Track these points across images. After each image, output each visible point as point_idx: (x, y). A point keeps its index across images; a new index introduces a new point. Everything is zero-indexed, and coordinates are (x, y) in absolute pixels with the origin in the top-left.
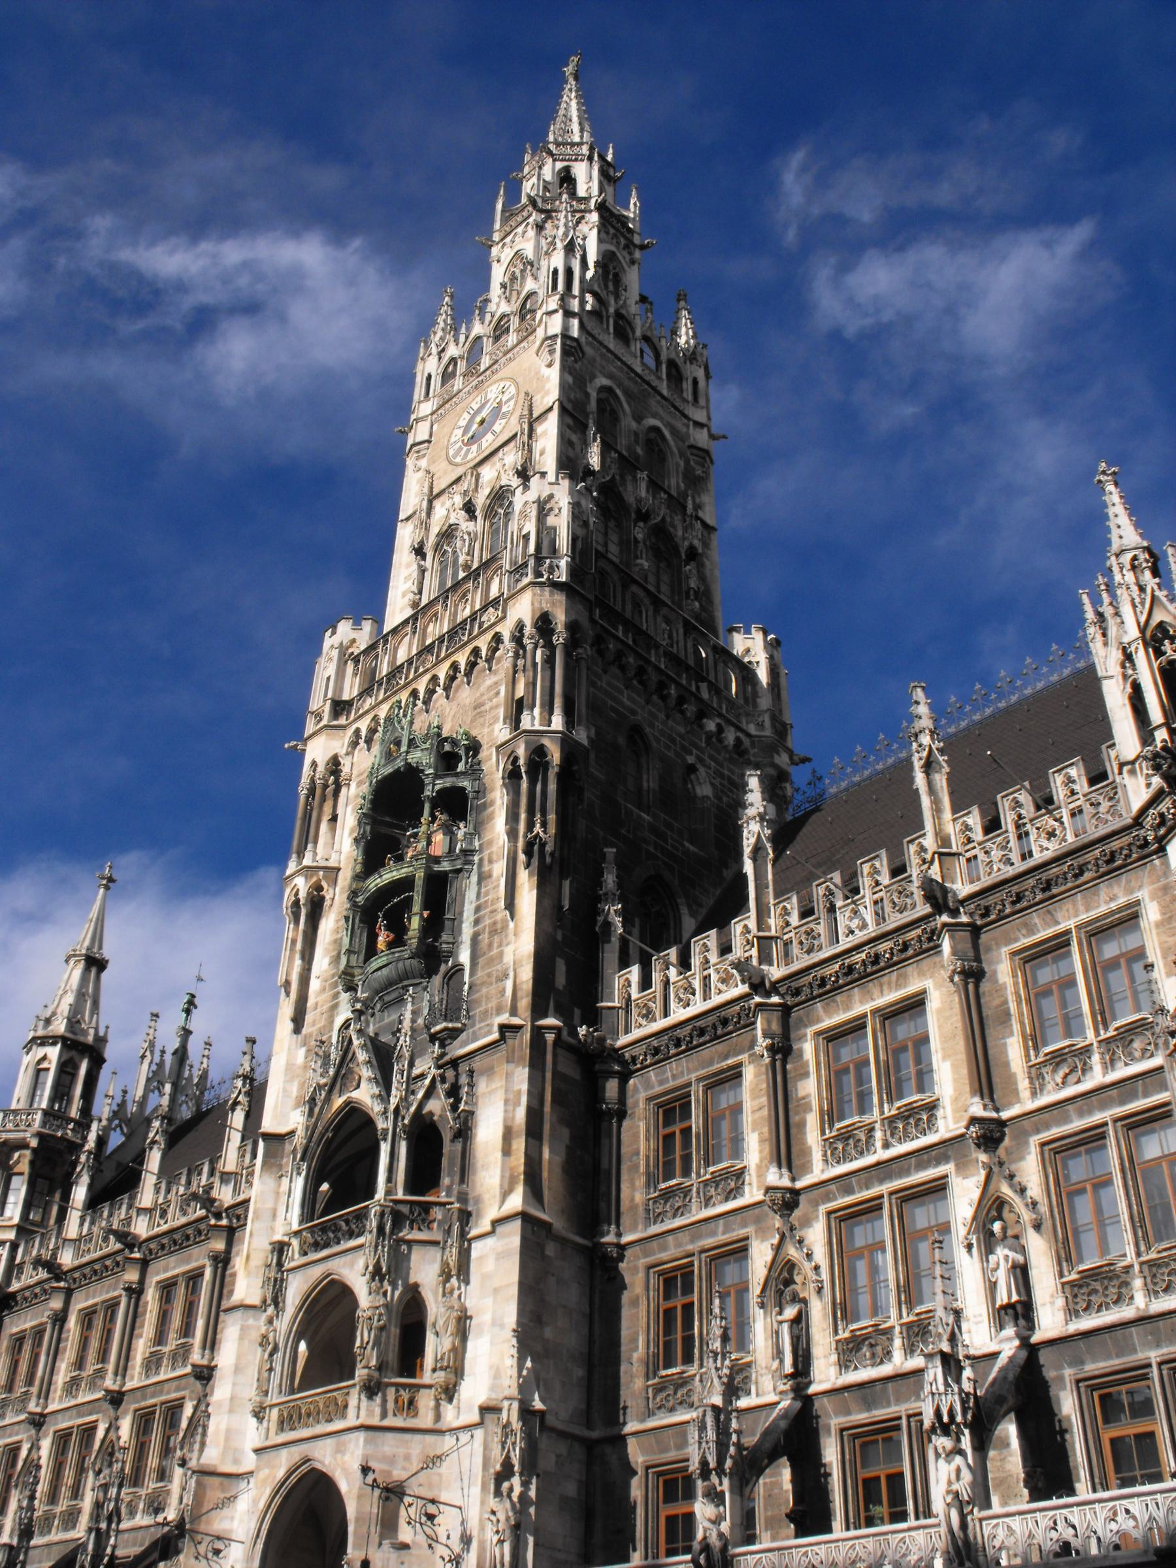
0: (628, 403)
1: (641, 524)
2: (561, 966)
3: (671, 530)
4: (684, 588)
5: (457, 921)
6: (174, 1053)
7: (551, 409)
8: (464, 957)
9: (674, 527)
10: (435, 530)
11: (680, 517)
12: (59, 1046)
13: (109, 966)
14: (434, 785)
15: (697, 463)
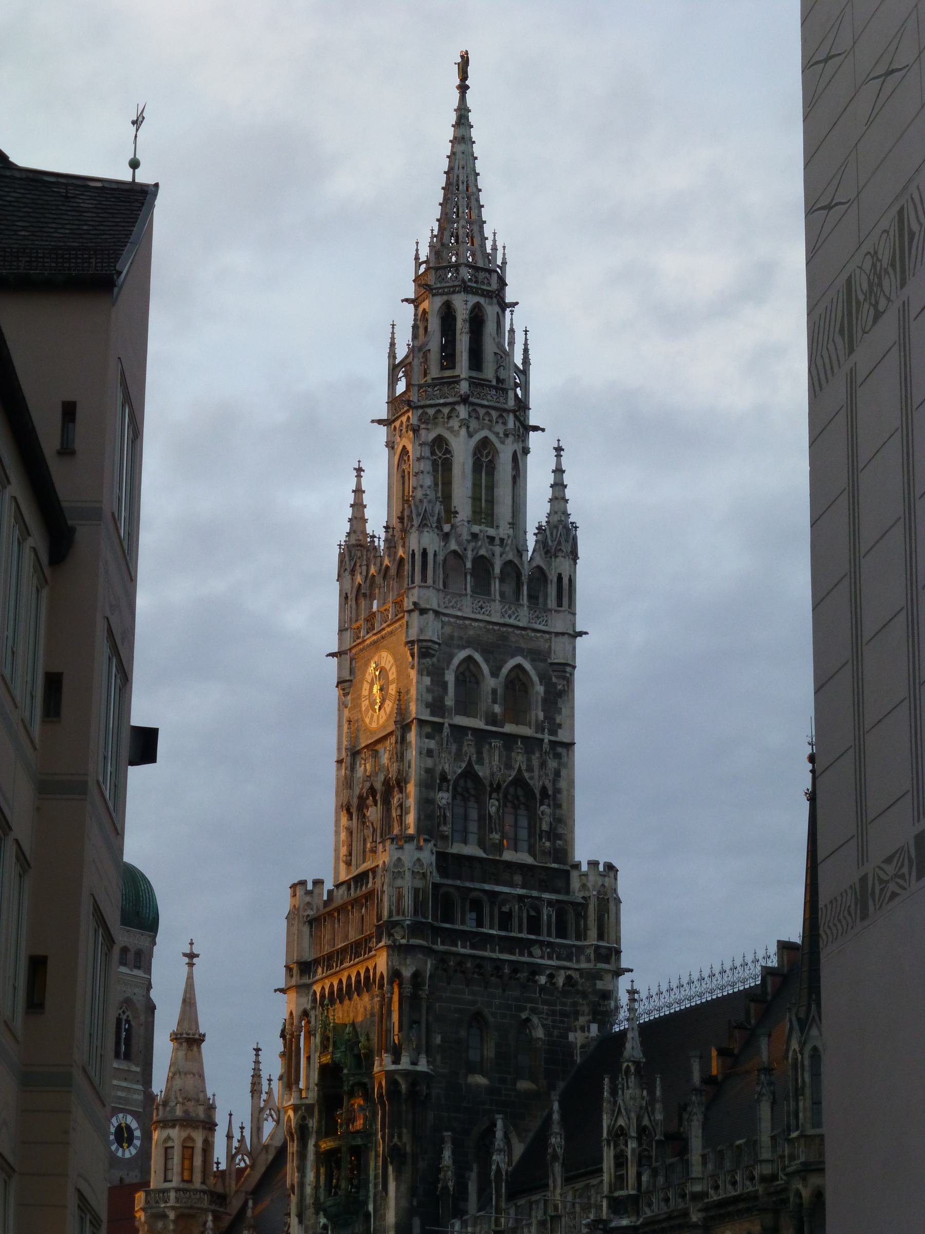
0: (487, 661)
1: (494, 795)
2: (417, 1222)
3: (526, 775)
4: (538, 831)
5: (367, 1181)
6: (281, 1078)
7: (412, 722)
8: (371, 1208)
9: (530, 769)
10: (357, 792)
11: (537, 754)
12: (177, 1128)
13: (207, 1038)
14: (349, 1081)
15: (557, 677)
